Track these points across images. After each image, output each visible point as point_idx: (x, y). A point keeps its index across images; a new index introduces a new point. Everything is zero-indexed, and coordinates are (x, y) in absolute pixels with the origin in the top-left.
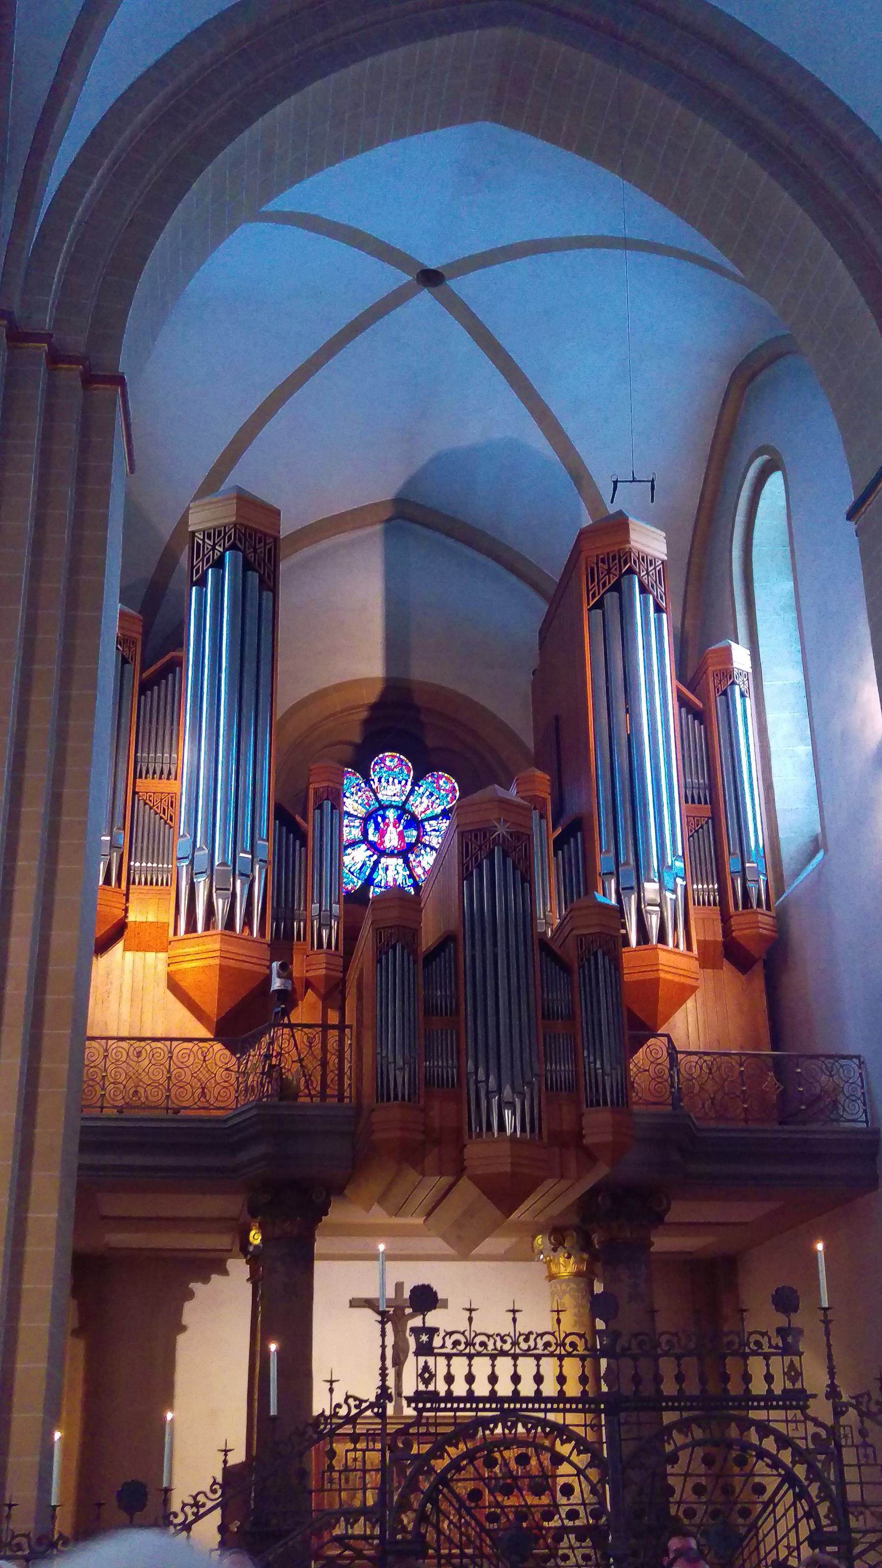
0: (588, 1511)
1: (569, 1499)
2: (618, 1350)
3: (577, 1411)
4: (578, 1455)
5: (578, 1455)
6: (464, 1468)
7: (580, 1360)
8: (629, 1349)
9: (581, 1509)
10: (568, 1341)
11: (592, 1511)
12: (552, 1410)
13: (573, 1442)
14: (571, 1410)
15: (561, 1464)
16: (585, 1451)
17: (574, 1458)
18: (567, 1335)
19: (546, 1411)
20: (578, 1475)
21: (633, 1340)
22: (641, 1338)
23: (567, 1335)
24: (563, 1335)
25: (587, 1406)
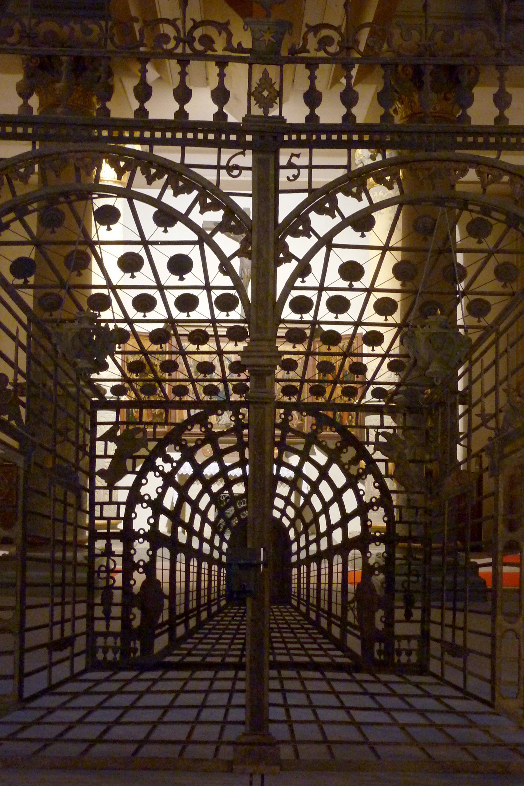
0: (214, 298)
1: (182, 279)
2: (284, 53)
3: (205, 143)
4: (202, 212)
5: (202, 212)
6: (7, 226)
7: (217, 64)
8: (304, 49)
9: (202, 295)
10: (198, 33)
11: (218, 299)
12: (164, 142)
13: (195, 193)
14: (195, 143)
15: (172, 224)
16: (215, 207)
17: (196, 216)
18: (196, 25)
19: (152, 142)
20: (200, 243)
21: (311, 35)
22: (324, 32)
23: (196, 25)
24: (189, 24)
25: (223, 137)
